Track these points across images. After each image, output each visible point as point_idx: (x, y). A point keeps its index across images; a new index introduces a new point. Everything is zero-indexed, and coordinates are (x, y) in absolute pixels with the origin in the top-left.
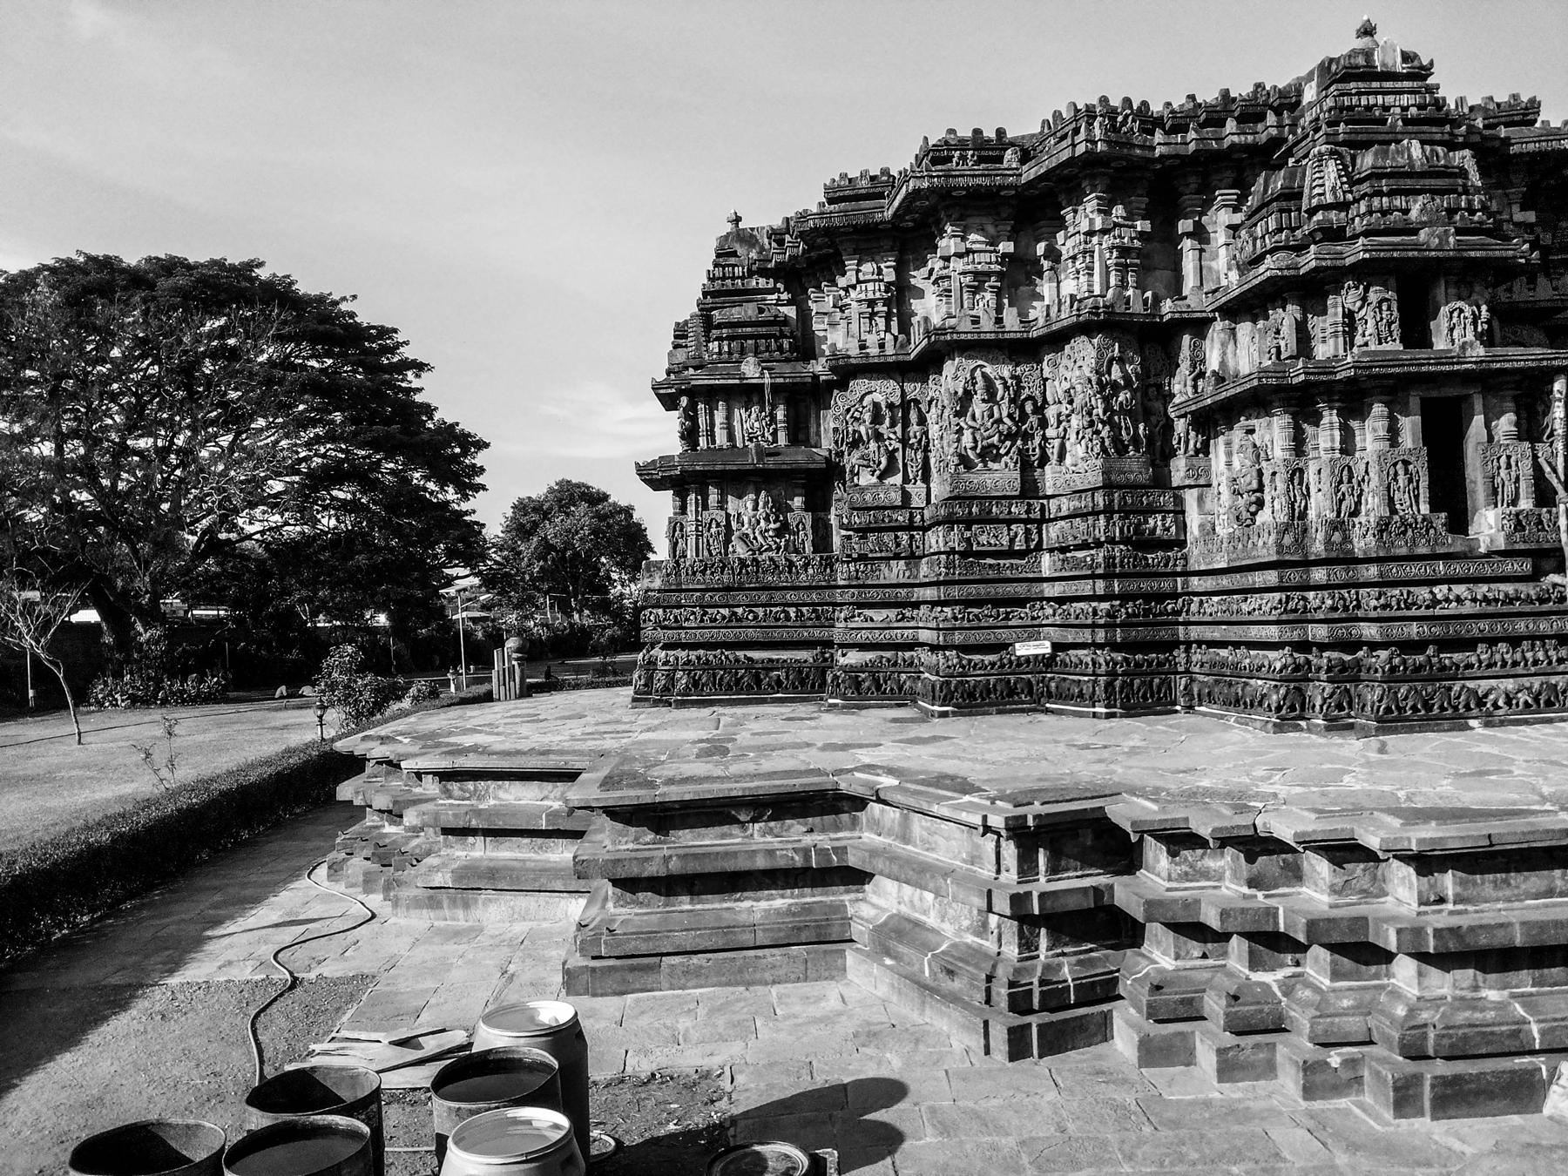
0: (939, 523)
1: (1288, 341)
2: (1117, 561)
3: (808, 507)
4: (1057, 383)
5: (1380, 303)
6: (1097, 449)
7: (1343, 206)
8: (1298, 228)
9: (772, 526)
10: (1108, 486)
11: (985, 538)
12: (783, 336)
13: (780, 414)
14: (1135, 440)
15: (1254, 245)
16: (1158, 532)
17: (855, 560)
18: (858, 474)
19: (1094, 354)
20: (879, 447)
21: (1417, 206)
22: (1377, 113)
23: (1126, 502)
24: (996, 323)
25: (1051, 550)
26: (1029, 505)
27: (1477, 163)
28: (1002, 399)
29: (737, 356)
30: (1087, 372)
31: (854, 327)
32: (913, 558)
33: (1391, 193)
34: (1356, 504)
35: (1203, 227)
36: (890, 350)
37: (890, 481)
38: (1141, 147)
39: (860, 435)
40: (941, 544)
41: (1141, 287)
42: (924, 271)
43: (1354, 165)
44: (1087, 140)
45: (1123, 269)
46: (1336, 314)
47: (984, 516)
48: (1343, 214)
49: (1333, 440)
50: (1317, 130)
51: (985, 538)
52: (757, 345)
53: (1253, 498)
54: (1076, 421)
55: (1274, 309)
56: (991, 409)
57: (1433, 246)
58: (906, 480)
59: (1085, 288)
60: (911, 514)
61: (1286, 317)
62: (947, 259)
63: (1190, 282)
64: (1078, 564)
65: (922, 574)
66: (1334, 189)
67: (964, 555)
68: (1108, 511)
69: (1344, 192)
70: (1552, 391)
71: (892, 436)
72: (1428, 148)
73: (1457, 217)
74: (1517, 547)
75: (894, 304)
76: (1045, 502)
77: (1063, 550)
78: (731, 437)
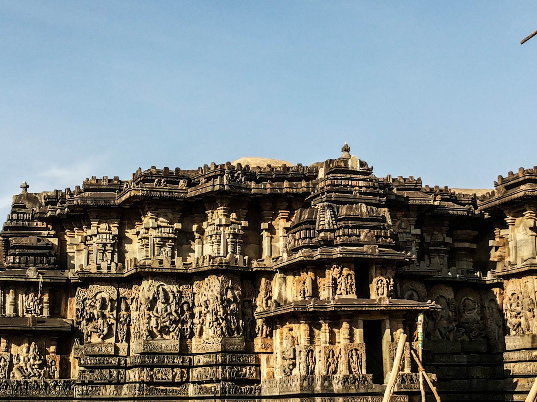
0: (136, 367)
1: (308, 286)
2: (227, 390)
3: (57, 353)
4: (200, 296)
5: (349, 274)
6: (219, 332)
7: (333, 231)
8: (314, 237)
9: (37, 362)
10: (224, 352)
11: (161, 375)
12: (51, 255)
13: (46, 298)
14: (238, 329)
15: (295, 243)
16: (247, 375)
17: (86, 384)
18: (90, 336)
19: (219, 285)
20: (104, 322)
21: (363, 234)
22: (349, 189)
23: (232, 360)
24: (171, 264)
25: (194, 383)
26: (184, 358)
27: (390, 214)
28: (172, 302)
29: (24, 265)
30: (216, 293)
31: (93, 257)
32: (119, 384)
33: (353, 227)
34: (335, 367)
35: (273, 226)
36: (113, 271)
37: (108, 341)
38: (245, 189)
39: (94, 315)
40: (137, 377)
41: (243, 254)
42: (134, 231)
43: (338, 212)
44: (220, 185)
45: (234, 244)
46: (329, 278)
47: (160, 363)
48: (333, 234)
49: (326, 337)
50: (323, 194)
51: (161, 375)
52: (35, 260)
53: (291, 363)
54: (209, 317)
55: (303, 272)
56: (166, 307)
57: (369, 253)
58: (117, 340)
59: (216, 251)
60: (119, 359)
61: (308, 277)
62: (147, 229)
63: (266, 253)
64: (208, 390)
65: (123, 393)
66: (329, 223)
67: (148, 384)
68: (224, 364)
69: (333, 225)
70: (417, 321)
71: (111, 316)
72: (369, 207)
73: (380, 240)
74: (402, 390)
75: (116, 247)
76: (192, 357)
77: (200, 383)
78: (16, 310)
